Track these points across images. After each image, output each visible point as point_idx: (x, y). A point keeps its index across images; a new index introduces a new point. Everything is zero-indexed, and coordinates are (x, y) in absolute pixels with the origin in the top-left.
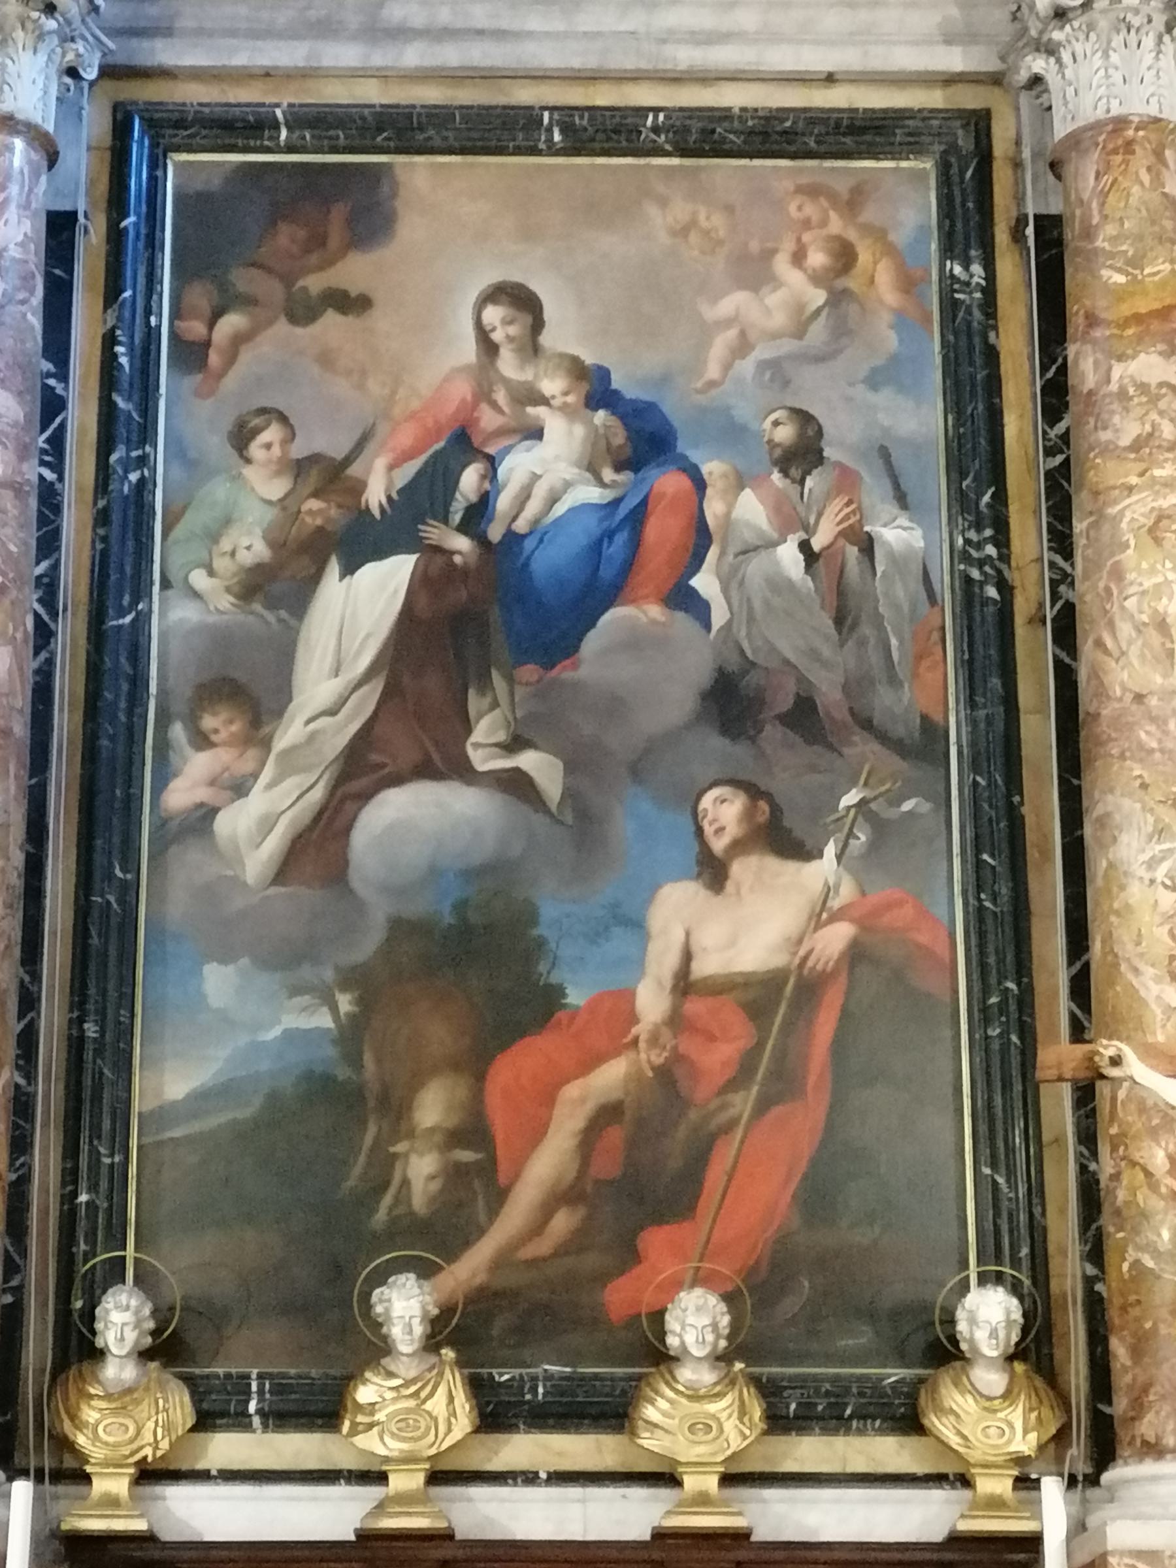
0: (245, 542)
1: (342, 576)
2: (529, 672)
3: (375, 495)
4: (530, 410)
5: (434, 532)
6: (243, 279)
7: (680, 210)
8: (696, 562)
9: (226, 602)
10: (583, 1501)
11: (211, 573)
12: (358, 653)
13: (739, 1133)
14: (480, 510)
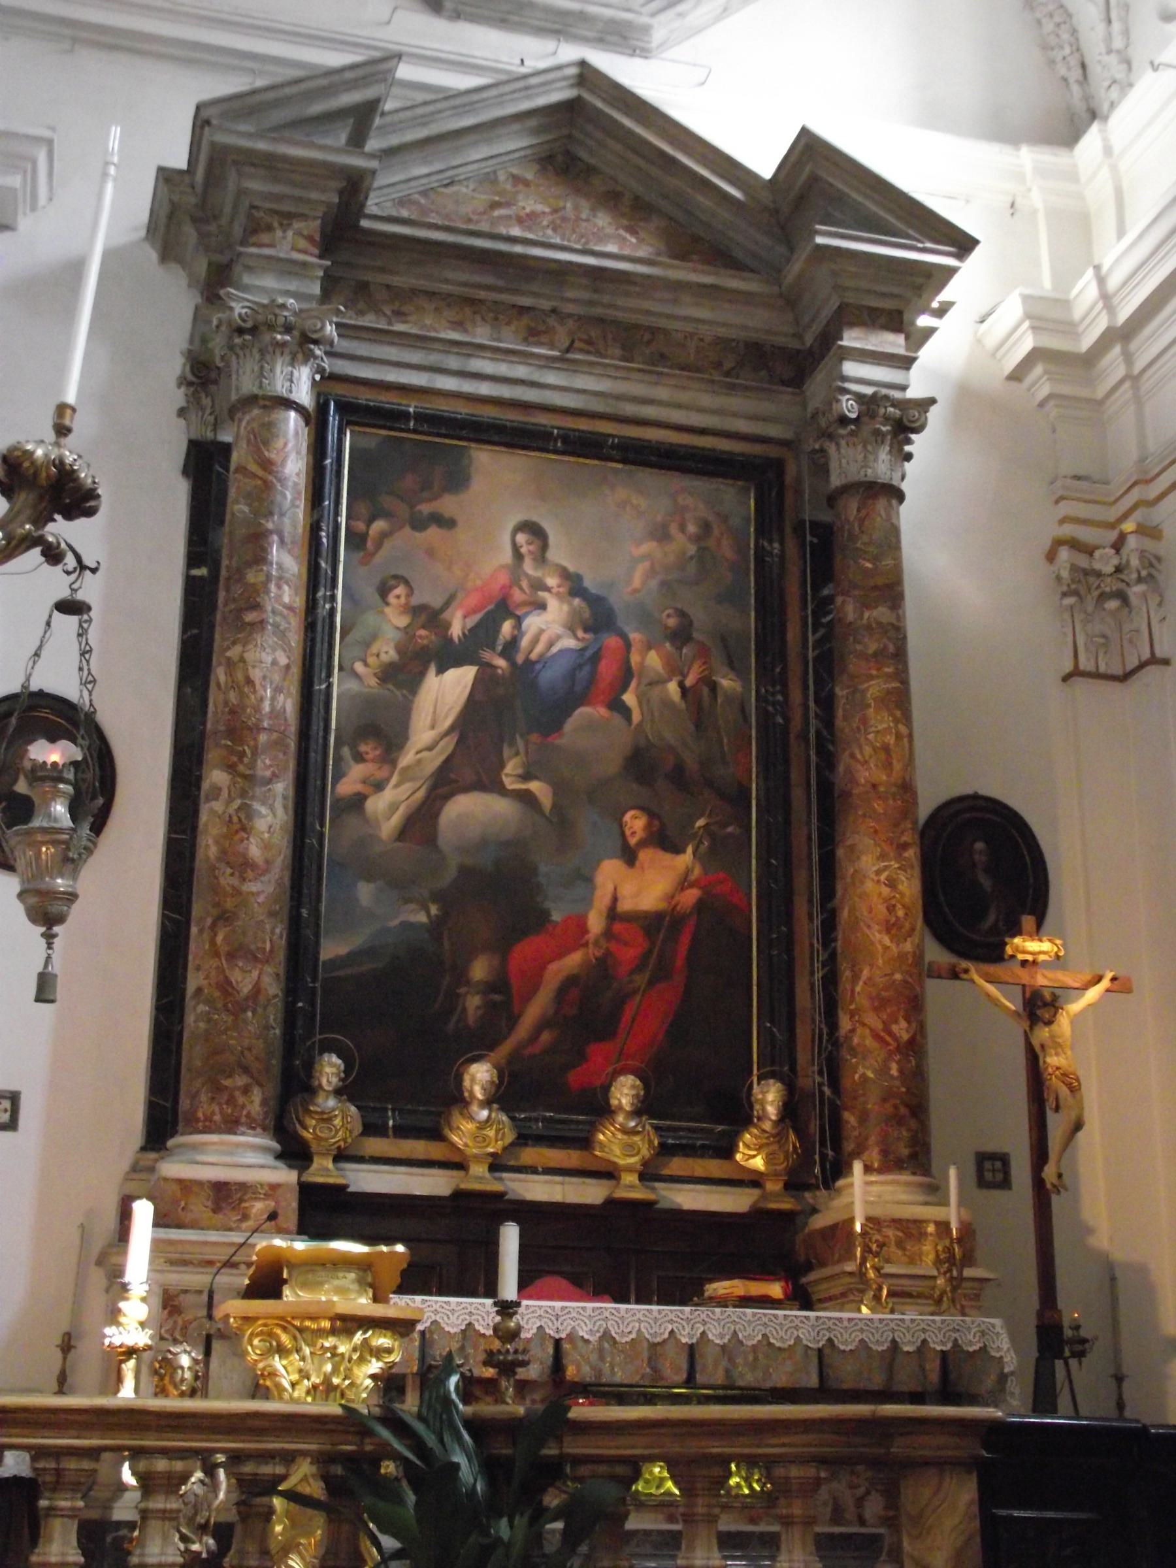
0: (385, 649)
1: (437, 674)
2: (534, 738)
4: (541, 594)
5: (487, 655)
6: (387, 501)
8: (624, 688)
9: (373, 681)
10: (562, 1183)
11: (366, 664)
12: (446, 717)
13: (638, 998)
14: (512, 645)
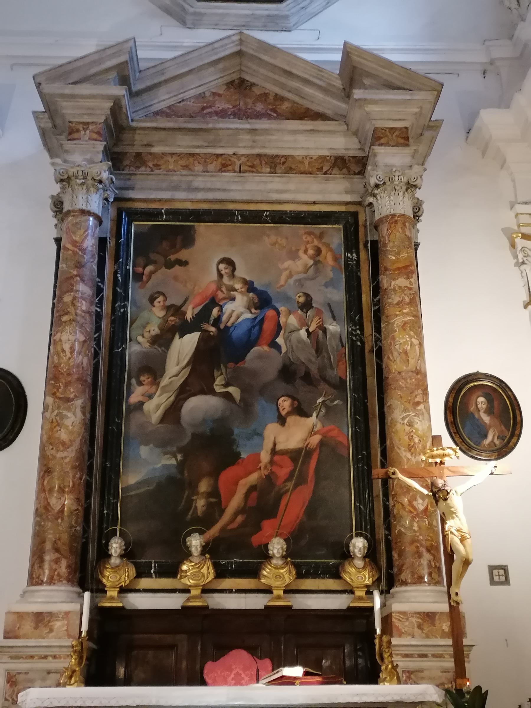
0: (153, 328)
1: (179, 338)
2: (231, 365)
3: (189, 316)
4: (232, 293)
5: (205, 326)
6: (153, 256)
7: (273, 238)
8: (277, 335)
9: (147, 345)
10: (245, 598)
11: (143, 337)
12: (184, 359)
13: (289, 494)
14: (218, 320)
